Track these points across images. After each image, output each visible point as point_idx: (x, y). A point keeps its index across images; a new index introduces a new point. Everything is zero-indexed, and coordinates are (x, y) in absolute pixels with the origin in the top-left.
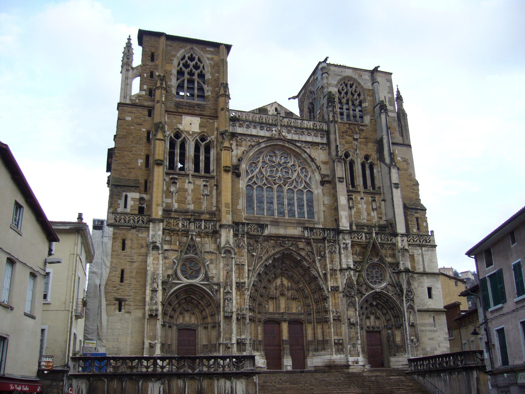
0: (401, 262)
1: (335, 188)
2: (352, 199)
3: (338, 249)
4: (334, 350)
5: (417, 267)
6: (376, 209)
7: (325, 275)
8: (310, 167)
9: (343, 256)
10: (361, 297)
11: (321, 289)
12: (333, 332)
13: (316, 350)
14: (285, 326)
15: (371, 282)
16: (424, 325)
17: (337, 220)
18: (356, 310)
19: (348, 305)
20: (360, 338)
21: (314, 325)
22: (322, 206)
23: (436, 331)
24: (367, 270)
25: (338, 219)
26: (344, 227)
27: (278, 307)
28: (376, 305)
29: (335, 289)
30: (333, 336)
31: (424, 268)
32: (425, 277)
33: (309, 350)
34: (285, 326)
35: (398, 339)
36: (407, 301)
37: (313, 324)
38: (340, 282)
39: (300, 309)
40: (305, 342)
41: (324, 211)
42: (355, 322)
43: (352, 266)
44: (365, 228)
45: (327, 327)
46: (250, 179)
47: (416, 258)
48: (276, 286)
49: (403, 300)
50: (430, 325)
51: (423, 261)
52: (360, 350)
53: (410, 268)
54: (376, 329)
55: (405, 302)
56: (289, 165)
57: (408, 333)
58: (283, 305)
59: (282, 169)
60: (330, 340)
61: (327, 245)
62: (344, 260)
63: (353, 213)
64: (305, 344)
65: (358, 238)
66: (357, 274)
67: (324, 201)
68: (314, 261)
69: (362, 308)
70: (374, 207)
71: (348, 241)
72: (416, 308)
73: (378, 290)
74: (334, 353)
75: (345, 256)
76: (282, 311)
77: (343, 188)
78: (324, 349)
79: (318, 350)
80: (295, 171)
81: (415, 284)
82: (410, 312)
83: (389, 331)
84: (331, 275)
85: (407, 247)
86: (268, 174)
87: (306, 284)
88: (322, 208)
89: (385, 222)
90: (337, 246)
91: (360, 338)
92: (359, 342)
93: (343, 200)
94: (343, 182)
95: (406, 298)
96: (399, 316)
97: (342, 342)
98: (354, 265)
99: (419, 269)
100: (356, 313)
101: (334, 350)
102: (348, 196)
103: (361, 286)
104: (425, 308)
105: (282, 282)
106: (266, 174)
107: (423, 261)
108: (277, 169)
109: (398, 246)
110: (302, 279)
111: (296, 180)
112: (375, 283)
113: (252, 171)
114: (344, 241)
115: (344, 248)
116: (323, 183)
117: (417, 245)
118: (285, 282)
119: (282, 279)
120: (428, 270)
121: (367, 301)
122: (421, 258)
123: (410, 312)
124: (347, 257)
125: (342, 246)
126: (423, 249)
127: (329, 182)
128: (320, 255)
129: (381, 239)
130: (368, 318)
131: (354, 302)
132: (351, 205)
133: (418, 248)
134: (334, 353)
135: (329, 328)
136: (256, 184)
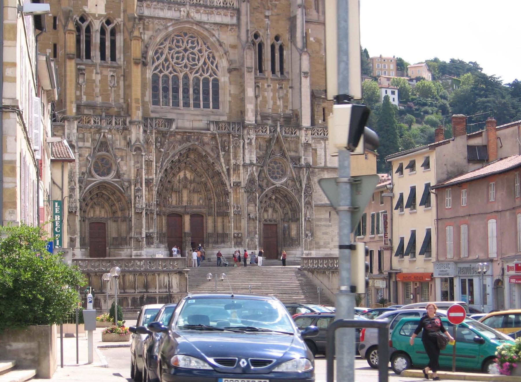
0: (303, 157)
1: (242, 76)
2: (258, 86)
3: (242, 144)
4: (233, 243)
5: (318, 161)
7: (228, 170)
9: (246, 151)
10: (262, 192)
11: (223, 184)
13: (216, 242)
14: (187, 219)
15: (272, 177)
16: (320, 220)
17: (242, 113)
18: (256, 205)
19: (249, 201)
20: (258, 232)
21: (215, 218)
22: (228, 95)
23: (331, 226)
24: (269, 166)
25: (244, 112)
27: (180, 200)
29: (237, 185)
31: (325, 162)
34: (187, 219)
35: (294, 233)
36: (306, 196)
39: (201, 202)
40: (205, 234)
41: (230, 102)
42: (254, 217)
43: (255, 162)
44: (270, 118)
47: (318, 152)
48: (179, 179)
50: (325, 220)
51: (325, 156)
52: (257, 243)
53: (311, 164)
55: (303, 198)
56: (196, 51)
57: (303, 228)
58: (185, 199)
59: (188, 56)
61: (231, 140)
63: (259, 103)
64: (205, 236)
65: (263, 132)
66: (259, 168)
67: (230, 91)
68: (218, 156)
69: (261, 202)
70: (281, 95)
71: (252, 136)
72: (313, 203)
73: (278, 185)
75: (249, 151)
76: (185, 204)
77: (251, 79)
78: (223, 242)
79: (217, 242)
80: (202, 56)
82: (308, 208)
84: (234, 170)
85: (310, 142)
88: (228, 98)
89: (291, 112)
90: (241, 141)
91: (258, 232)
92: (257, 236)
93: (250, 92)
94: (251, 72)
95: (304, 193)
96: (296, 210)
97: (242, 236)
98: (257, 160)
99: (321, 163)
100: (256, 209)
103: (263, 181)
104: (323, 203)
105: (185, 175)
107: (325, 156)
109: (301, 140)
112: (276, 178)
113: (158, 59)
114: (249, 136)
116: (230, 71)
117: (321, 138)
118: (188, 175)
119: (185, 172)
120: (329, 165)
121: (266, 196)
122: (323, 152)
123: (308, 208)
124: (250, 152)
127: (235, 69)
129: (286, 133)
133: (322, 141)
134: (233, 246)
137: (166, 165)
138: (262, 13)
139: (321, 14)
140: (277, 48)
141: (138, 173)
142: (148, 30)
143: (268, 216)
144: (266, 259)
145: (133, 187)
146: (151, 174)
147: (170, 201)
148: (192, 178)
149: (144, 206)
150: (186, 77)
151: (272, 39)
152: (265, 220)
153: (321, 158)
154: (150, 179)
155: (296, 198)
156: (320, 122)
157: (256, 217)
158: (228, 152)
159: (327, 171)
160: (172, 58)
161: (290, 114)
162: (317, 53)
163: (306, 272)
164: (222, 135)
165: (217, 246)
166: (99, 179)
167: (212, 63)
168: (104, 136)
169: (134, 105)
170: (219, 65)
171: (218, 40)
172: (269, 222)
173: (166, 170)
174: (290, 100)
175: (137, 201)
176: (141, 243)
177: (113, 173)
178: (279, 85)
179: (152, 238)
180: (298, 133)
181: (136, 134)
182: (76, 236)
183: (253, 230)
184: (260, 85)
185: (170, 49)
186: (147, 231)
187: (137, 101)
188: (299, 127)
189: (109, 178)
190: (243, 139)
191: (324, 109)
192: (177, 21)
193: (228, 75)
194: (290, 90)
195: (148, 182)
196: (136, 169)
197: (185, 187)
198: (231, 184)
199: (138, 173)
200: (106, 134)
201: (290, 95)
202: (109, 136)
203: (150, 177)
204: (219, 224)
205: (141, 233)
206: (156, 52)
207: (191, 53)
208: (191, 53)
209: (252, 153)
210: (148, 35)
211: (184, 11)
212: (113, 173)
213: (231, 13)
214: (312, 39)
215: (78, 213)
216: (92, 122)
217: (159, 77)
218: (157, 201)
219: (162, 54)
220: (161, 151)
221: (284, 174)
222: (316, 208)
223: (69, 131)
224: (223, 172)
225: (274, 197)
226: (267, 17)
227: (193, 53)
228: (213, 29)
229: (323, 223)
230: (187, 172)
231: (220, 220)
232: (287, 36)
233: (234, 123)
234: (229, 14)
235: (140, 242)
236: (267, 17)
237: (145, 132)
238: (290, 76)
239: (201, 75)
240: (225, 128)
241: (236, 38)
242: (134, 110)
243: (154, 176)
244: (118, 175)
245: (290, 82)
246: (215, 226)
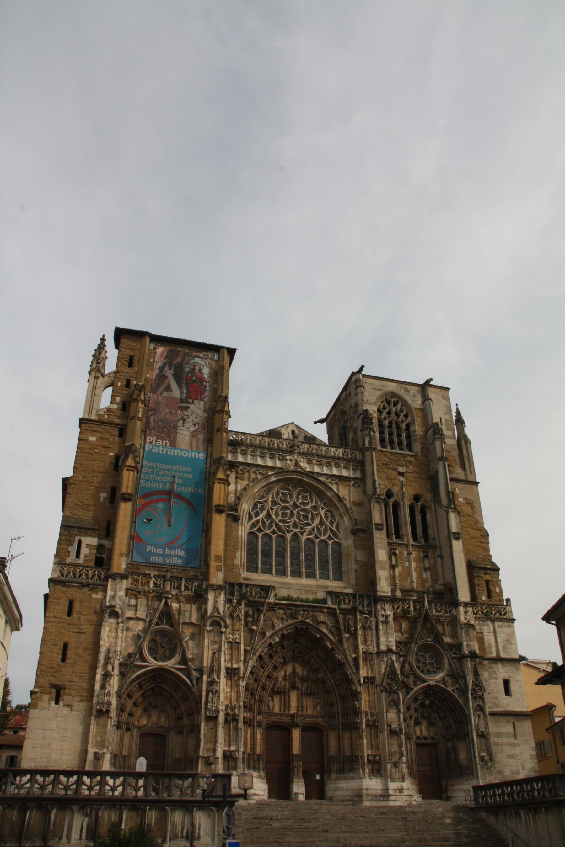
0: (465, 643)
1: (371, 538)
2: (395, 554)
3: (374, 624)
4: (367, 771)
6: (429, 569)
7: (356, 660)
8: (337, 509)
9: (381, 633)
10: (408, 693)
11: (349, 681)
12: (365, 744)
13: (341, 771)
14: (296, 734)
15: (422, 671)
16: (499, 735)
17: (373, 582)
18: (399, 711)
19: (389, 706)
20: (405, 753)
21: (339, 734)
22: (353, 562)
23: (518, 745)
24: (417, 654)
25: (376, 581)
26: (384, 592)
27: (286, 705)
28: (430, 705)
29: (370, 681)
30: (365, 750)
31: (498, 651)
32: (499, 665)
33: (330, 770)
34: (296, 734)
35: (462, 756)
36: (475, 699)
37: (337, 732)
38: (377, 671)
39: (319, 709)
41: (356, 571)
42: (397, 729)
43: (394, 648)
45: (358, 736)
46: (254, 525)
48: (285, 675)
49: (468, 698)
50: (508, 735)
52: (405, 771)
54: (430, 741)
55: (471, 701)
56: (308, 507)
58: (294, 703)
59: (298, 512)
60: (362, 757)
61: (359, 617)
62: (382, 639)
63: (397, 574)
64: (325, 762)
66: (402, 659)
67: (356, 557)
68: (340, 641)
69: (408, 708)
70: (427, 565)
71: (388, 613)
72: (487, 710)
73: (431, 683)
74: (367, 776)
75: (384, 633)
76: (293, 711)
78: (352, 770)
79: (344, 770)
80: (317, 514)
81: (485, 675)
82: (479, 716)
83: (449, 745)
84: (365, 660)
86: (280, 518)
87: (328, 673)
88: (354, 566)
90: (373, 619)
91: (405, 753)
92: (404, 759)
95: (472, 694)
96: (462, 720)
97: (380, 760)
98: (397, 647)
100: (399, 717)
101: (367, 771)
102: (391, 549)
103: (408, 677)
104: (501, 709)
105: (294, 669)
106: (276, 518)
108: (291, 512)
109: (460, 621)
110: (323, 666)
111: (317, 527)
112: (429, 672)
113: (257, 514)
114: (383, 613)
115: (383, 622)
118: (299, 670)
119: (294, 665)
120: (503, 655)
121: (416, 699)
122: (493, 637)
123: (479, 716)
124: (386, 633)
125: (381, 619)
126: (496, 624)
127: (362, 531)
128: (349, 632)
129: (437, 611)
130: (417, 723)
131: (396, 700)
132: (394, 563)
134: (367, 776)
135: (361, 737)
136: (262, 531)
137: (261, 649)
138: (394, 469)
139: (468, 473)
140: (417, 509)
141: (216, 657)
142: (242, 479)
143: (421, 731)
144: (423, 798)
145: (205, 678)
146: (238, 662)
147: (271, 706)
148: (305, 673)
149: (222, 707)
150: (296, 537)
151: (410, 499)
152: (418, 738)
153: (490, 645)
154: (235, 669)
155: (461, 701)
156: (484, 598)
157: (401, 730)
158: (354, 635)
159: (502, 664)
160: (277, 514)
161: (442, 590)
162: (470, 516)
163: (483, 814)
164: (344, 612)
165: (343, 776)
166: (153, 663)
167: (332, 523)
168: (166, 603)
169: (213, 564)
170: (340, 526)
171: (337, 495)
172: (423, 741)
173: (260, 657)
174: (440, 572)
175: (210, 699)
176: (213, 766)
177: (177, 657)
178: (423, 552)
179: (236, 759)
180: (454, 612)
181: (216, 601)
182: (105, 750)
183: (397, 750)
184: (397, 552)
185: (274, 503)
186: (226, 748)
187: (218, 558)
188: (456, 604)
189: (171, 664)
190: (376, 617)
191: (487, 582)
192: (281, 471)
193: (353, 537)
194: (439, 560)
195: (232, 673)
196: (211, 652)
197: (293, 687)
198: (360, 681)
199: (216, 657)
200: (169, 601)
201: (439, 566)
202: (175, 605)
203: (235, 666)
204: (347, 742)
205: (214, 751)
206: (255, 506)
207: (301, 510)
208: (301, 510)
209: (389, 636)
210: (242, 485)
211: (291, 460)
212: (177, 657)
213: (353, 465)
214: (461, 500)
215: (113, 714)
216: (152, 585)
217: (257, 537)
218: (245, 702)
219: (263, 509)
220: (252, 630)
221: (439, 668)
222: (492, 717)
223: (112, 593)
224: (348, 662)
225: (427, 702)
226: (401, 474)
227: (303, 510)
228: (330, 483)
229: (505, 740)
230: (296, 665)
231: (347, 735)
232: (428, 496)
233: (361, 596)
234: (351, 467)
235: (211, 764)
236: (401, 474)
237: (229, 601)
238: (437, 543)
239: (316, 537)
240: (349, 601)
241: (361, 493)
242: (212, 570)
243: (241, 665)
244: (184, 660)
245: (438, 550)
246: (339, 746)
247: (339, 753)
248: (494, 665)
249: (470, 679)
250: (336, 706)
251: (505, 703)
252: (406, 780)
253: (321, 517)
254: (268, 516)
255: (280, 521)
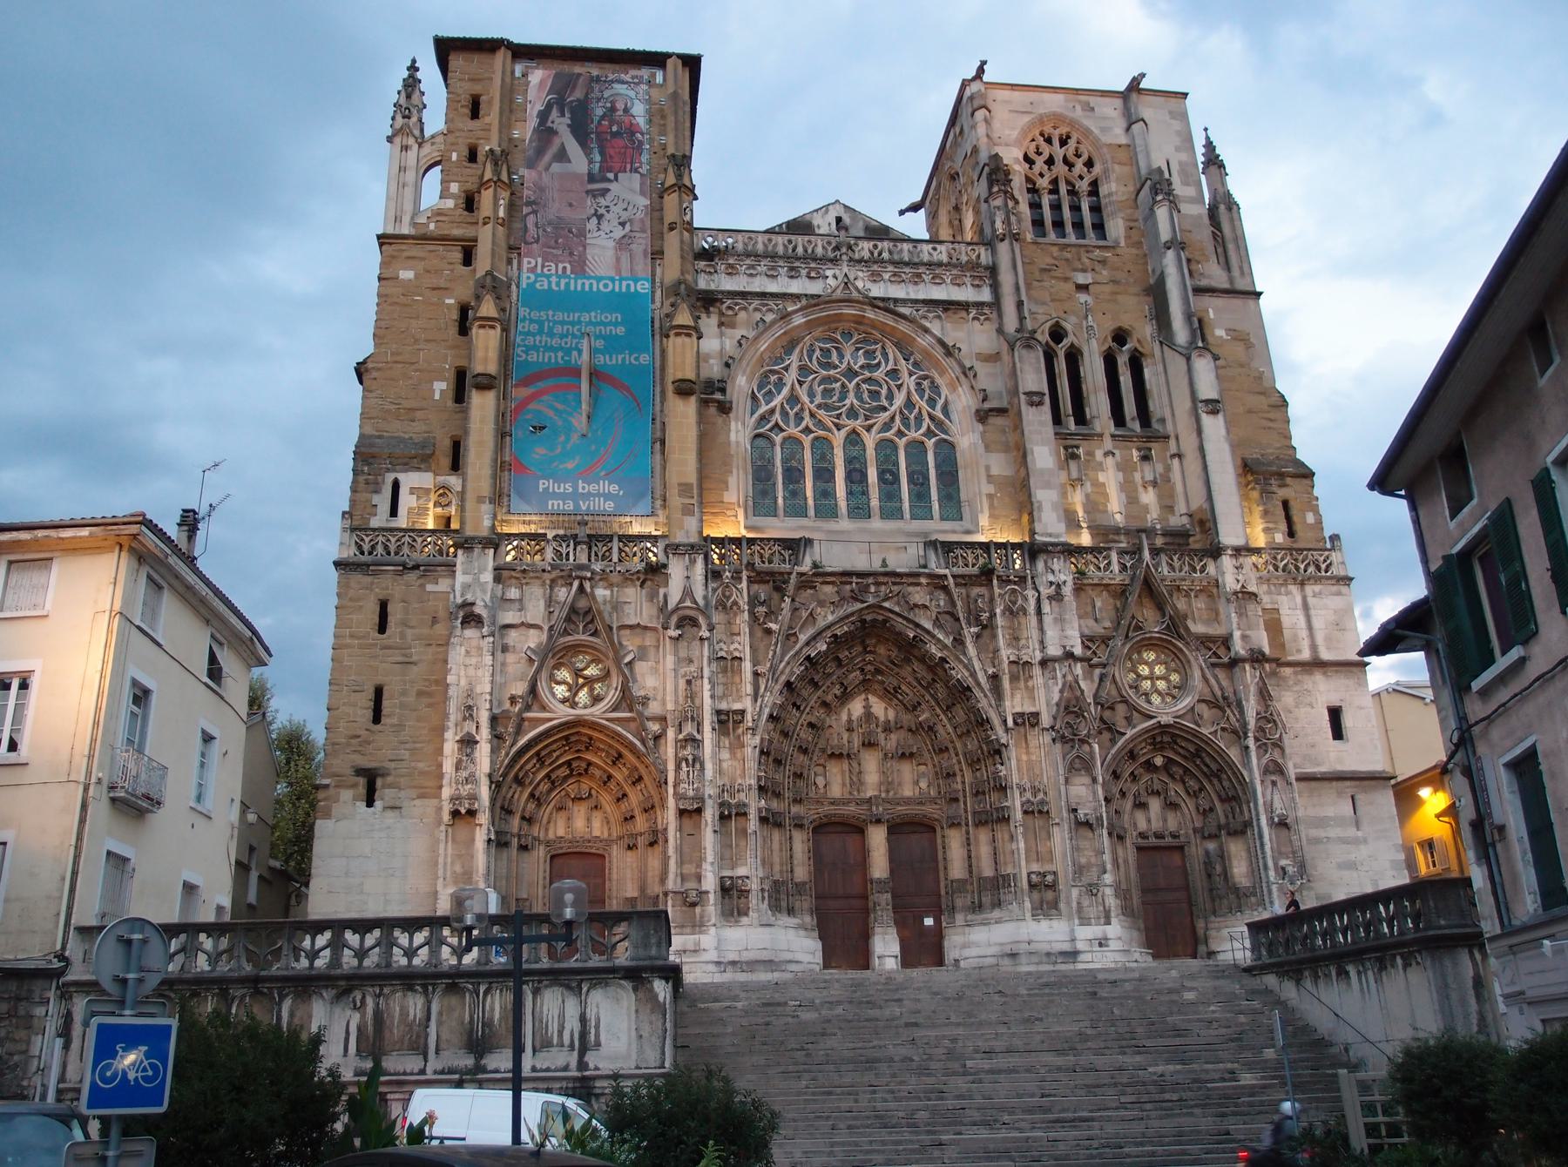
0: (1237, 634)
1: (1018, 426)
2: (1074, 457)
4: (1028, 905)
13: (977, 907)
14: (877, 838)
16: (1322, 822)
20: (1109, 867)
27: (857, 781)
30: (1023, 863)
31: (1314, 647)
36: (1263, 748)
39: (924, 784)
40: (942, 885)
45: (1007, 837)
50: (1340, 821)
51: (1310, 627)
52: (1112, 902)
53: (1267, 650)
59: (858, 385)
64: (943, 892)
67: (988, 468)
72: (1292, 773)
78: (998, 904)
79: (980, 906)
80: (899, 387)
81: (1285, 700)
82: (1274, 783)
85: (1252, 588)
86: (818, 400)
91: (1109, 867)
95: (1257, 739)
96: (1236, 795)
100: (1095, 793)
104: (1323, 769)
107: (1310, 627)
113: (769, 396)
123: (1274, 783)
127: (1002, 411)
134: (1028, 915)
148: (891, 715)
150: (853, 439)
157: (1099, 819)
160: (811, 395)
165: (979, 917)
167: (932, 402)
170: (951, 407)
180: (1211, 569)
185: (804, 370)
193: (980, 427)
197: (869, 744)
204: (984, 851)
207: (864, 381)
208: (864, 381)
219: (780, 384)
222: (1303, 784)
227: (869, 380)
229: (1333, 832)
231: (983, 836)
239: (900, 434)
247: (971, 872)
248: (1306, 677)
249: (1251, 708)
250: (959, 779)
251: (1332, 755)
252: (1114, 920)
253: (909, 393)
254: (793, 399)
255: (819, 406)
